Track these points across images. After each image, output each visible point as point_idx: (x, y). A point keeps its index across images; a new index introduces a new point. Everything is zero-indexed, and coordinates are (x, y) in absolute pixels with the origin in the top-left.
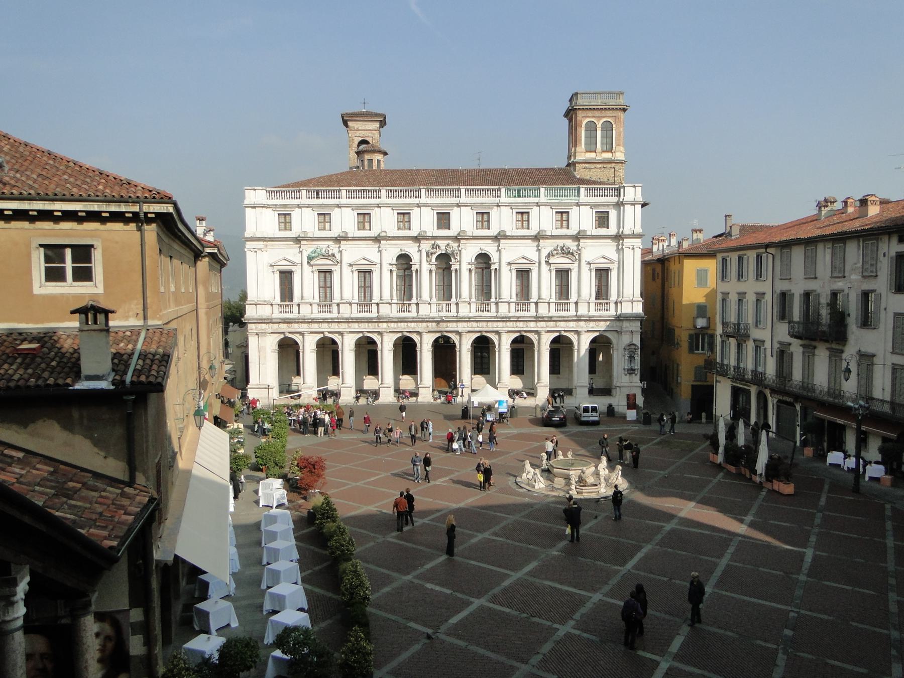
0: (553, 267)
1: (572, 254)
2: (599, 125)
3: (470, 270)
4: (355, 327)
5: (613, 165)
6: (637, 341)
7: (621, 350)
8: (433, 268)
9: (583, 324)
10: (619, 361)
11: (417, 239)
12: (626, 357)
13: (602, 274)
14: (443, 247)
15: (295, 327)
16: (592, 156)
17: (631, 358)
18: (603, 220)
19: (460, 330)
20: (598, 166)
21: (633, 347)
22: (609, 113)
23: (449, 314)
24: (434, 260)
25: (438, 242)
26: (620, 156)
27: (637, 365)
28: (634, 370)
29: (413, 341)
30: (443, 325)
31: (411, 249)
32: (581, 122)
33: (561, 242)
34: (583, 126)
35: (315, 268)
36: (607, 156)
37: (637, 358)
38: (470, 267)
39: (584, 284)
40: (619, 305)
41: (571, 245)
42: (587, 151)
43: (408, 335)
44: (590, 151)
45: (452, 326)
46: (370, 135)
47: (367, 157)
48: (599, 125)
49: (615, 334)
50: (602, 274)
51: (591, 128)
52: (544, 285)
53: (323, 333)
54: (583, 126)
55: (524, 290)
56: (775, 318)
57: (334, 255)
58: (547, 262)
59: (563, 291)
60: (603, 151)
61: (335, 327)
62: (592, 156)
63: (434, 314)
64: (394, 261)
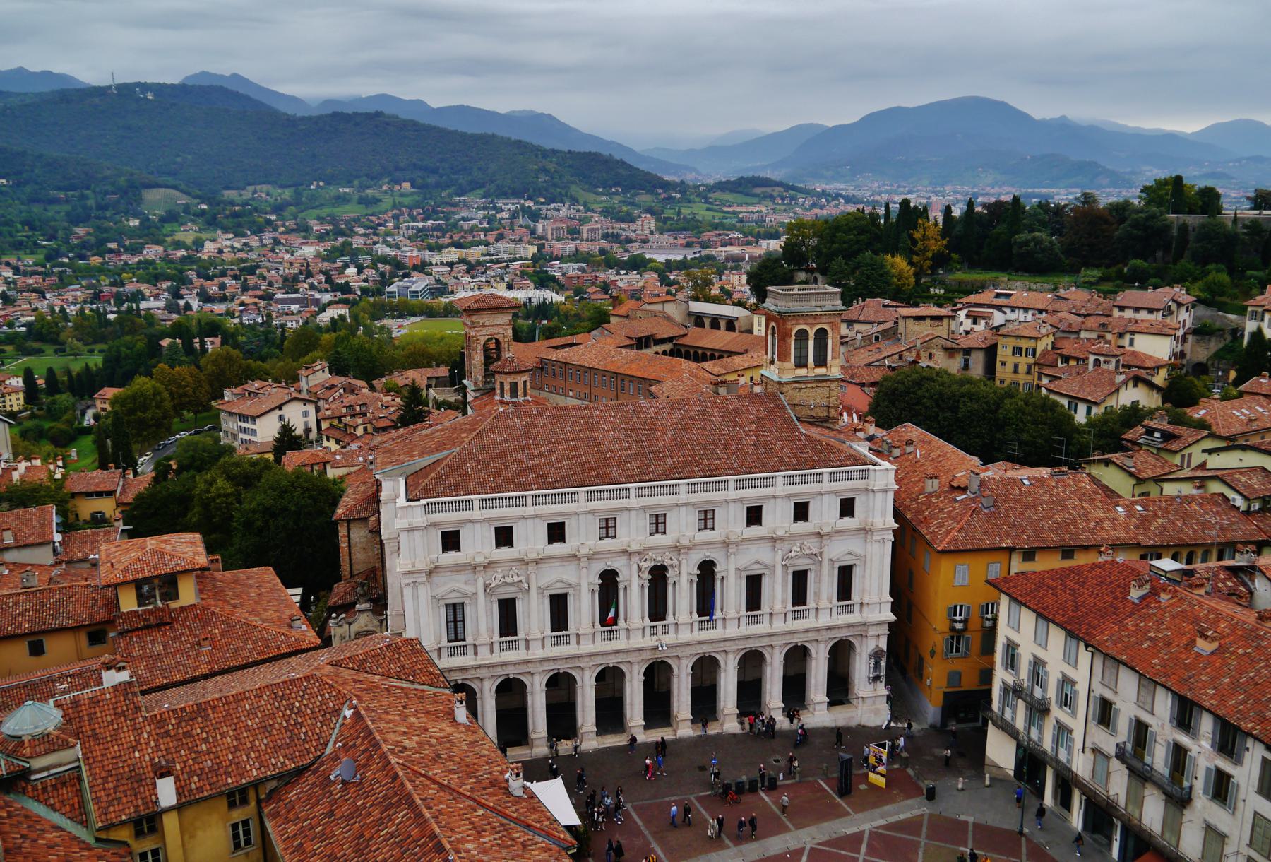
0: (791, 570)
6: (883, 644)
7: (865, 657)
8: (647, 584)
10: (861, 668)
26: (835, 372)
27: (883, 674)
31: (618, 564)
32: (791, 330)
37: (883, 663)
46: (501, 331)
52: (777, 592)
55: (754, 599)
56: (1090, 717)
59: (799, 596)
62: (802, 372)
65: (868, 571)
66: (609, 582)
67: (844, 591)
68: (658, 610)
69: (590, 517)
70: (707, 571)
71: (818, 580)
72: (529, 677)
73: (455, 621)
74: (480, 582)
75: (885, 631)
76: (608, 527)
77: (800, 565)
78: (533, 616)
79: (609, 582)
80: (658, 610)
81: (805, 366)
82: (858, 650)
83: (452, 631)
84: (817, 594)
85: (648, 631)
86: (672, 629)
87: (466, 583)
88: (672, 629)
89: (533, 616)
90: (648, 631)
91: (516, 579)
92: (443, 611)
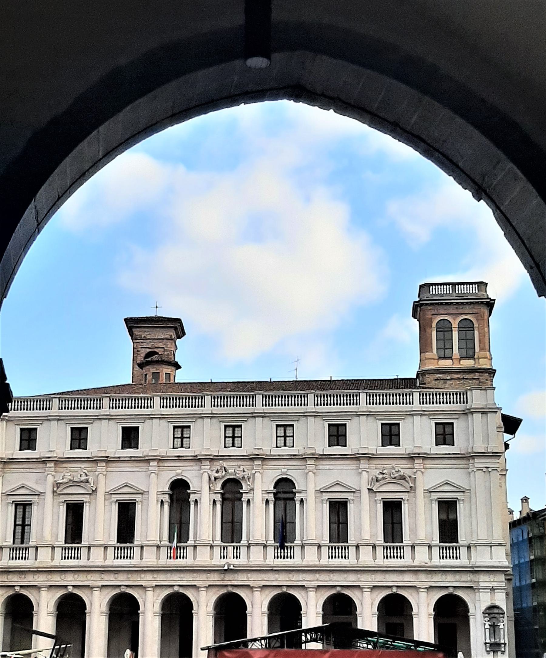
0: (379, 497)
1: (404, 479)
2: (455, 324)
3: (267, 502)
4: (110, 580)
5: (477, 375)
6: (501, 600)
8: (218, 498)
9: (422, 577)
11: (197, 459)
12: (487, 626)
13: (448, 508)
14: (231, 471)
15: (30, 580)
16: (446, 363)
17: (494, 628)
18: (444, 435)
19: (251, 584)
20: (456, 376)
21: (496, 611)
22: (467, 309)
23: (236, 562)
24: (218, 487)
25: (225, 464)
28: (499, 645)
29: (189, 599)
30: (229, 577)
32: (431, 321)
33: (388, 464)
34: (434, 325)
35: (63, 498)
36: (468, 363)
38: (267, 496)
39: (420, 521)
40: (472, 548)
41: (403, 468)
42: (440, 358)
43: (181, 590)
44: (445, 358)
45: (240, 579)
46: (161, 345)
47: (152, 369)
48: (455, 324)
49: (469, 591)
50: (448, 508)
51: (444, 329)
53: (66, 586)
54: (434, 325)
57: (87, 481)
60: (462, 358)
61: (81, 579)
63: (217, 561)
64: (167, 489)
65: (473, 507)
66: (179, 492)
67: (448, 531)
68: (232, 530)
69: (163, 423)
70: (284, 492)
71: (414, 514)
72: (87, 591)
73: (23, 526)
74: (50, 479)
75: (499, 581)
76: (182, 432)
77: (392, 492)
78: (100, 523)
79: (179, 492)
80: (232, 530)
81: (450, 358)
82: (472, 611)
83: (19, 536)
84: (414, 531)
85: (217, 550)
86: (243, 550)
87: (37, 483)
88: (243, 550)
89: (100, 523)
90: (217, 550)
91: (84, 478)
92: (12, 509)
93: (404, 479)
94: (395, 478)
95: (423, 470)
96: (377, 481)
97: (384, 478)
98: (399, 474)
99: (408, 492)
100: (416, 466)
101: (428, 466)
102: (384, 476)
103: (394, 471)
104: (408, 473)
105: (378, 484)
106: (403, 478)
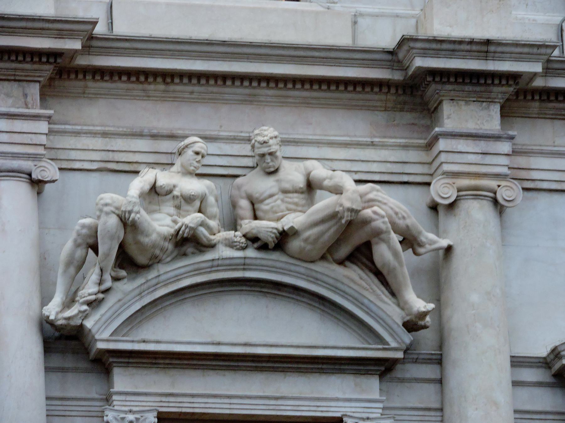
1: (362, 255)
41: (336, 165)
58: (63, 343)
93: (362, 255)
94: (283, 239)
95: (506, 192)
96: (128, 261)
97: (187, 242)
98: (324, 203)
99: (384, 368)
100: (457, 155)
101: (544, 168)
102: (192, 218)
103: (260, 185)
104: (389, 206)
105: (130, 292)
106: (353, 243)
